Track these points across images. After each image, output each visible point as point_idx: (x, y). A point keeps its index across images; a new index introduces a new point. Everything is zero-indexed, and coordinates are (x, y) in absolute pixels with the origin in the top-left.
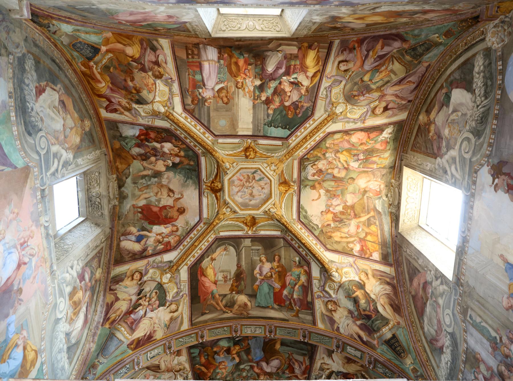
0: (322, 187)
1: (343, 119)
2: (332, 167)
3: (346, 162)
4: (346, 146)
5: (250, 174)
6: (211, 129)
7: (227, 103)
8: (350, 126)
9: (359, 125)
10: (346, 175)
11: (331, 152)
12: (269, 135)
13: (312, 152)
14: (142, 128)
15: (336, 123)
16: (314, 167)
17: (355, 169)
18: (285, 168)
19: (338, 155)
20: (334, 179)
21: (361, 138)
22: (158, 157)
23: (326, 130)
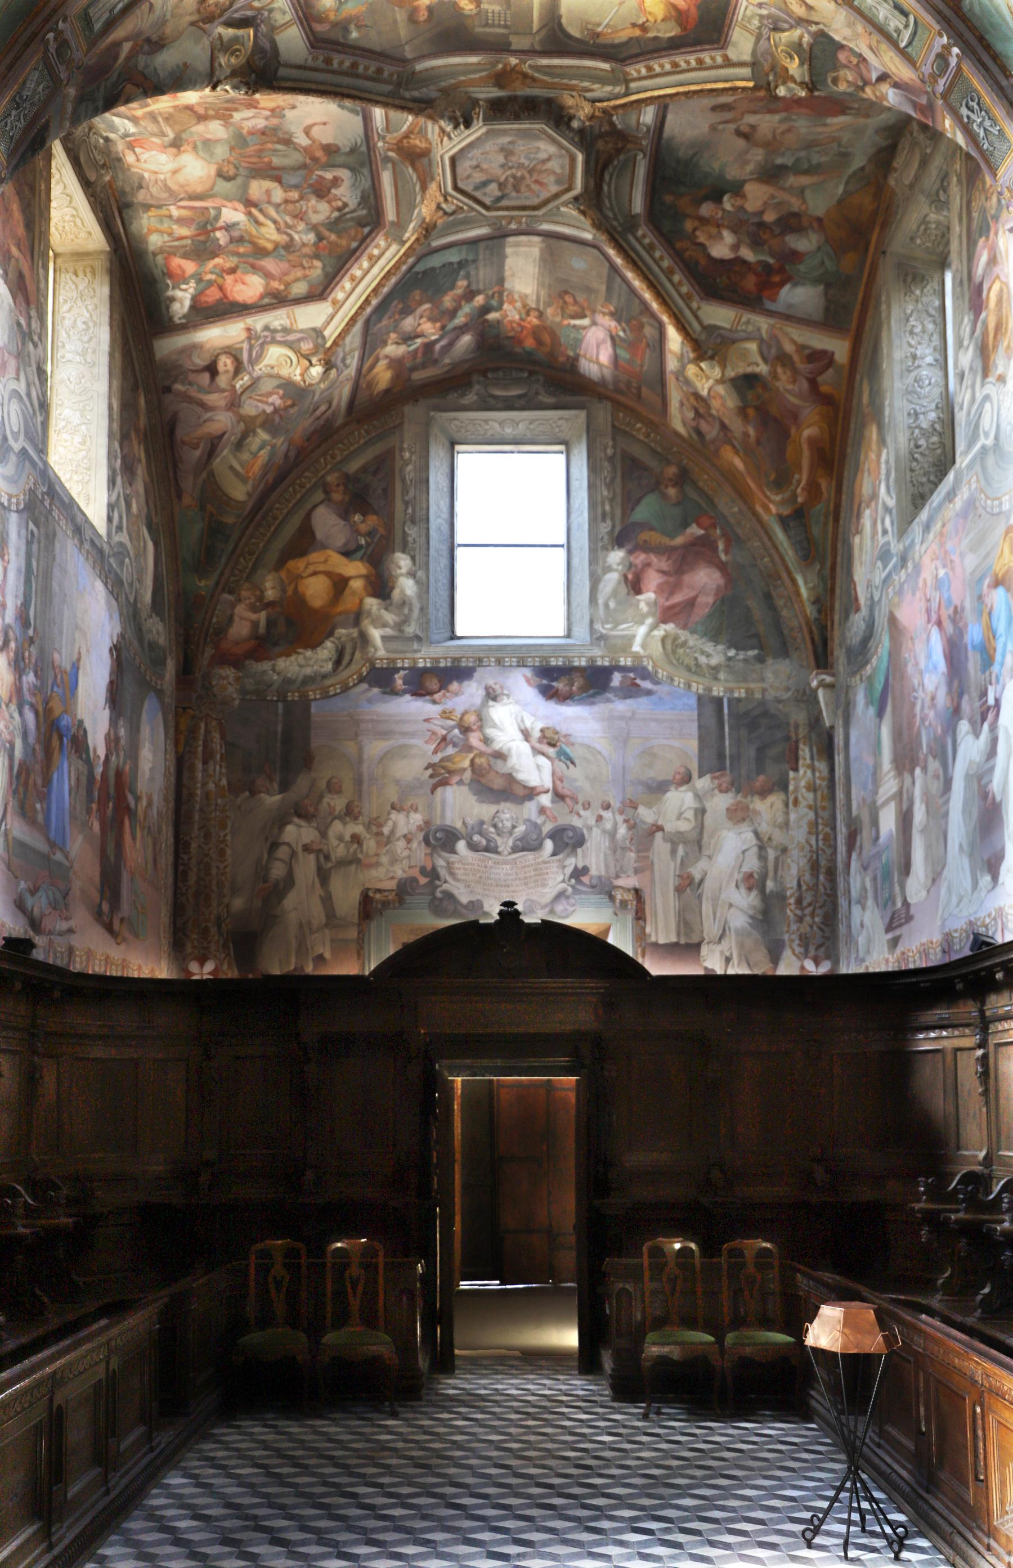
0: (306, 150)
1: (300, 340)
2: (290, 207)
3: (258, 223)
4: (269, 264)
5: (514, 194)
6: (607, 264)
7: (566, 292)
8: (277, 319)
9: (258, 322)
10: (245, 187)
11: (304, 245)
12: (464, 247)
13: (354, 245)
14: (769, 305)
15: (314, 329)
16: (340, 204)
17: (229, 204)
18: (418, 198)
19: (283, 239)
20: (275, 172)
21: (239, 287)
22: (755, 220)
23: (330, 310)
